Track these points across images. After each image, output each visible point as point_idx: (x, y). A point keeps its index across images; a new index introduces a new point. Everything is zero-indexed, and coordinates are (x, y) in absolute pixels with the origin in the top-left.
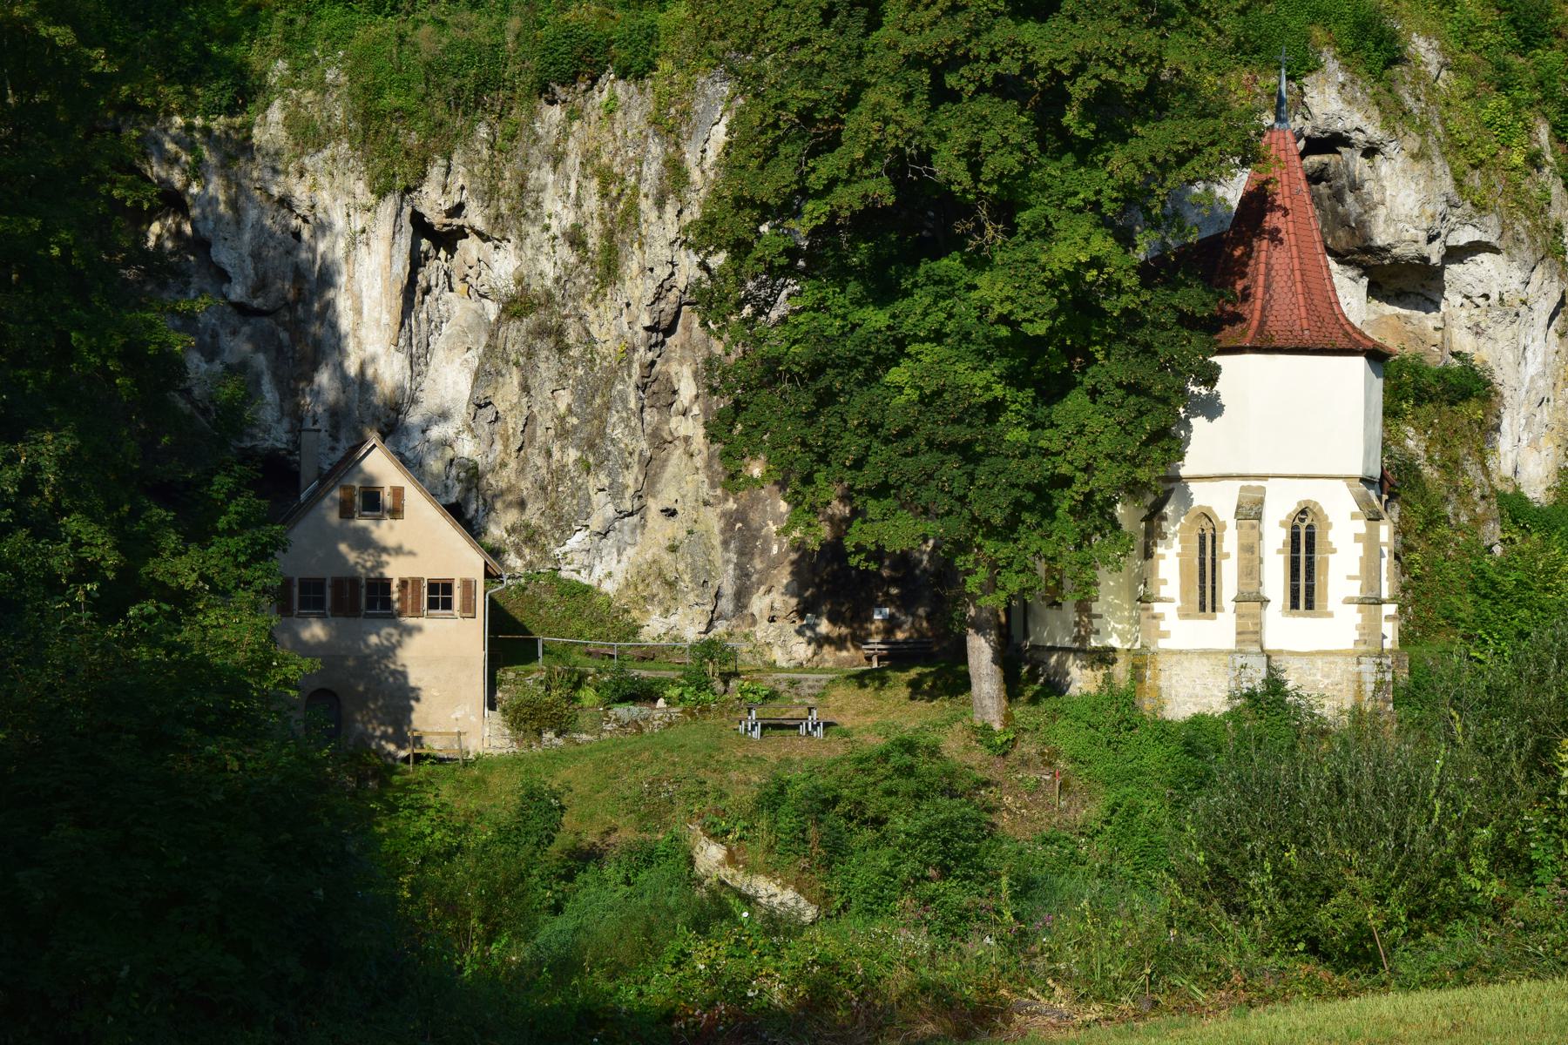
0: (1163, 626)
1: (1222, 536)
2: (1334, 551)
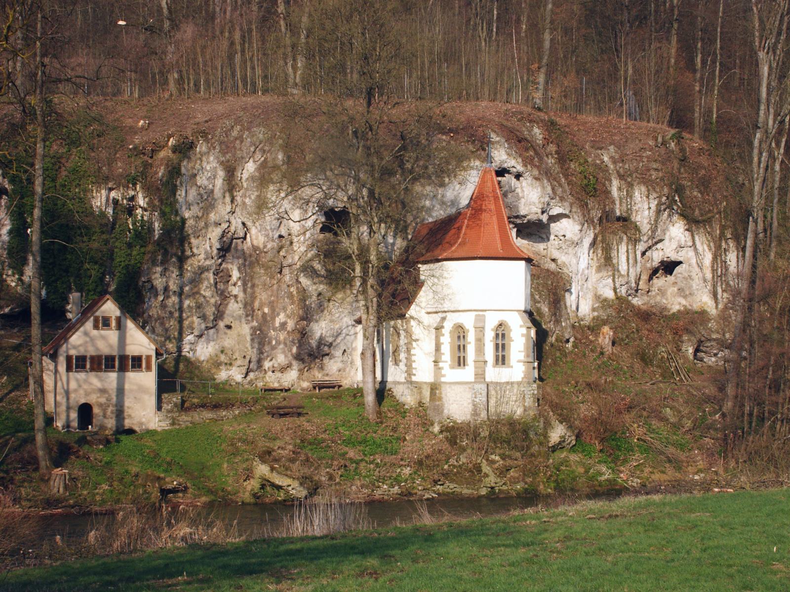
0: (443, 372)
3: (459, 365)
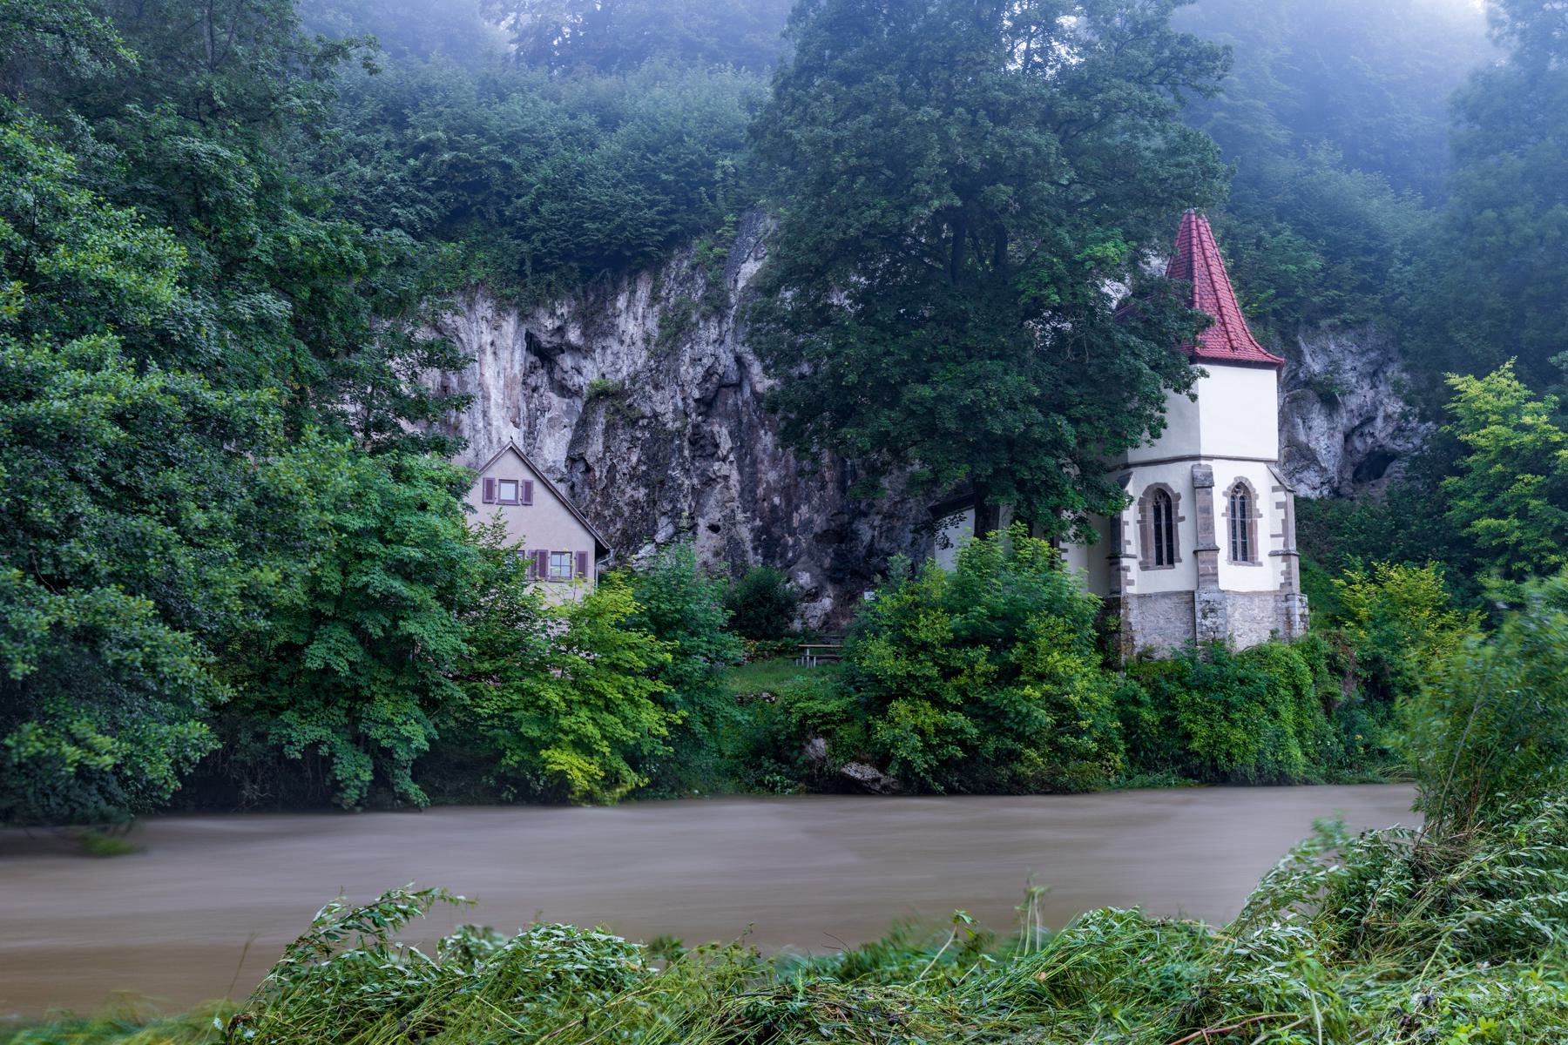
0: (1130, 576)
1: (1177, 505)
2: (1261, 516)
3: (1159, 562)
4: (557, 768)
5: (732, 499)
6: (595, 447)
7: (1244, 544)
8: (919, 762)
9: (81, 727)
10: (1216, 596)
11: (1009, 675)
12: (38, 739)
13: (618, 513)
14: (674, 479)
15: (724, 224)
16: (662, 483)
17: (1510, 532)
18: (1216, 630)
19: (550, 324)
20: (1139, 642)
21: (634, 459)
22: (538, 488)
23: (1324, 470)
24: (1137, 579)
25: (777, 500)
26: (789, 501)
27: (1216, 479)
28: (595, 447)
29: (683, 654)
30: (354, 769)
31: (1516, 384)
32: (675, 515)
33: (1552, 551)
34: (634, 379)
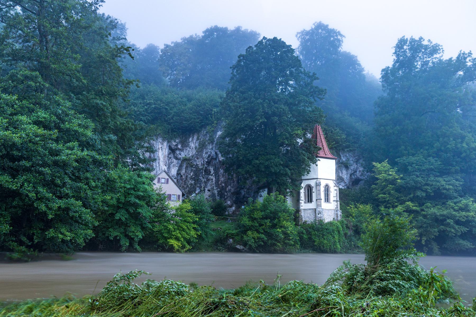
0: (302, 205)
3: (308, 202)
4: (171, 244)
5: (213, 184)
6: (183, 171)
7: (327, 198)
8: (253, 245)
9: (63, 230)
10: (321, 210)
11: (274, 226)
12: (53, 233)
13: (188, 186)
14: (200, 179)
15: (214, 123)
16: (198, 180)
17: (386, 198)
18: (321, 218)
19: (174, 144)
20: (304, 219)
21: (192, 174)
22: (170, 180)
23: (346, 182)
24: (304, 205)
25: (223, 185)
26: (226, 185)
27: (321, 183)
28: (183, 171)
29: (200, 219)
30: (125, 243)
31: (388, 165)
32: (200, 187)
33: (396, 202)
34: (192, 156)
